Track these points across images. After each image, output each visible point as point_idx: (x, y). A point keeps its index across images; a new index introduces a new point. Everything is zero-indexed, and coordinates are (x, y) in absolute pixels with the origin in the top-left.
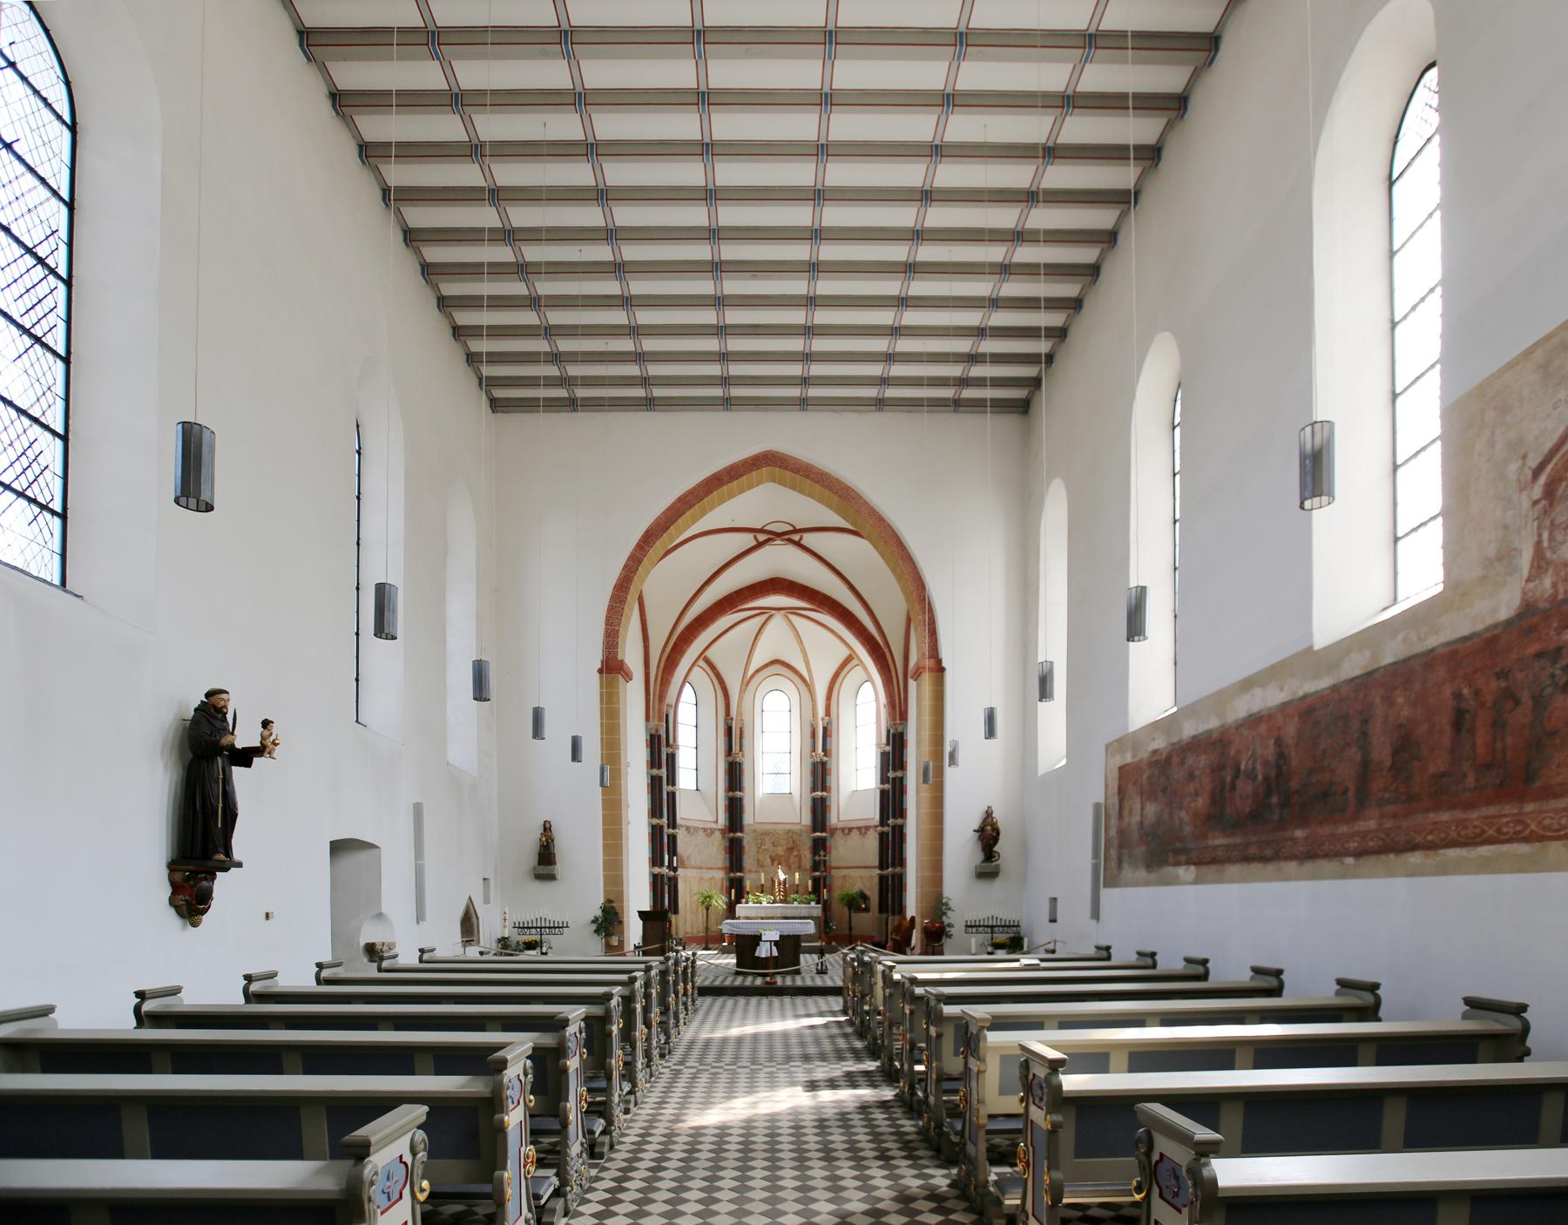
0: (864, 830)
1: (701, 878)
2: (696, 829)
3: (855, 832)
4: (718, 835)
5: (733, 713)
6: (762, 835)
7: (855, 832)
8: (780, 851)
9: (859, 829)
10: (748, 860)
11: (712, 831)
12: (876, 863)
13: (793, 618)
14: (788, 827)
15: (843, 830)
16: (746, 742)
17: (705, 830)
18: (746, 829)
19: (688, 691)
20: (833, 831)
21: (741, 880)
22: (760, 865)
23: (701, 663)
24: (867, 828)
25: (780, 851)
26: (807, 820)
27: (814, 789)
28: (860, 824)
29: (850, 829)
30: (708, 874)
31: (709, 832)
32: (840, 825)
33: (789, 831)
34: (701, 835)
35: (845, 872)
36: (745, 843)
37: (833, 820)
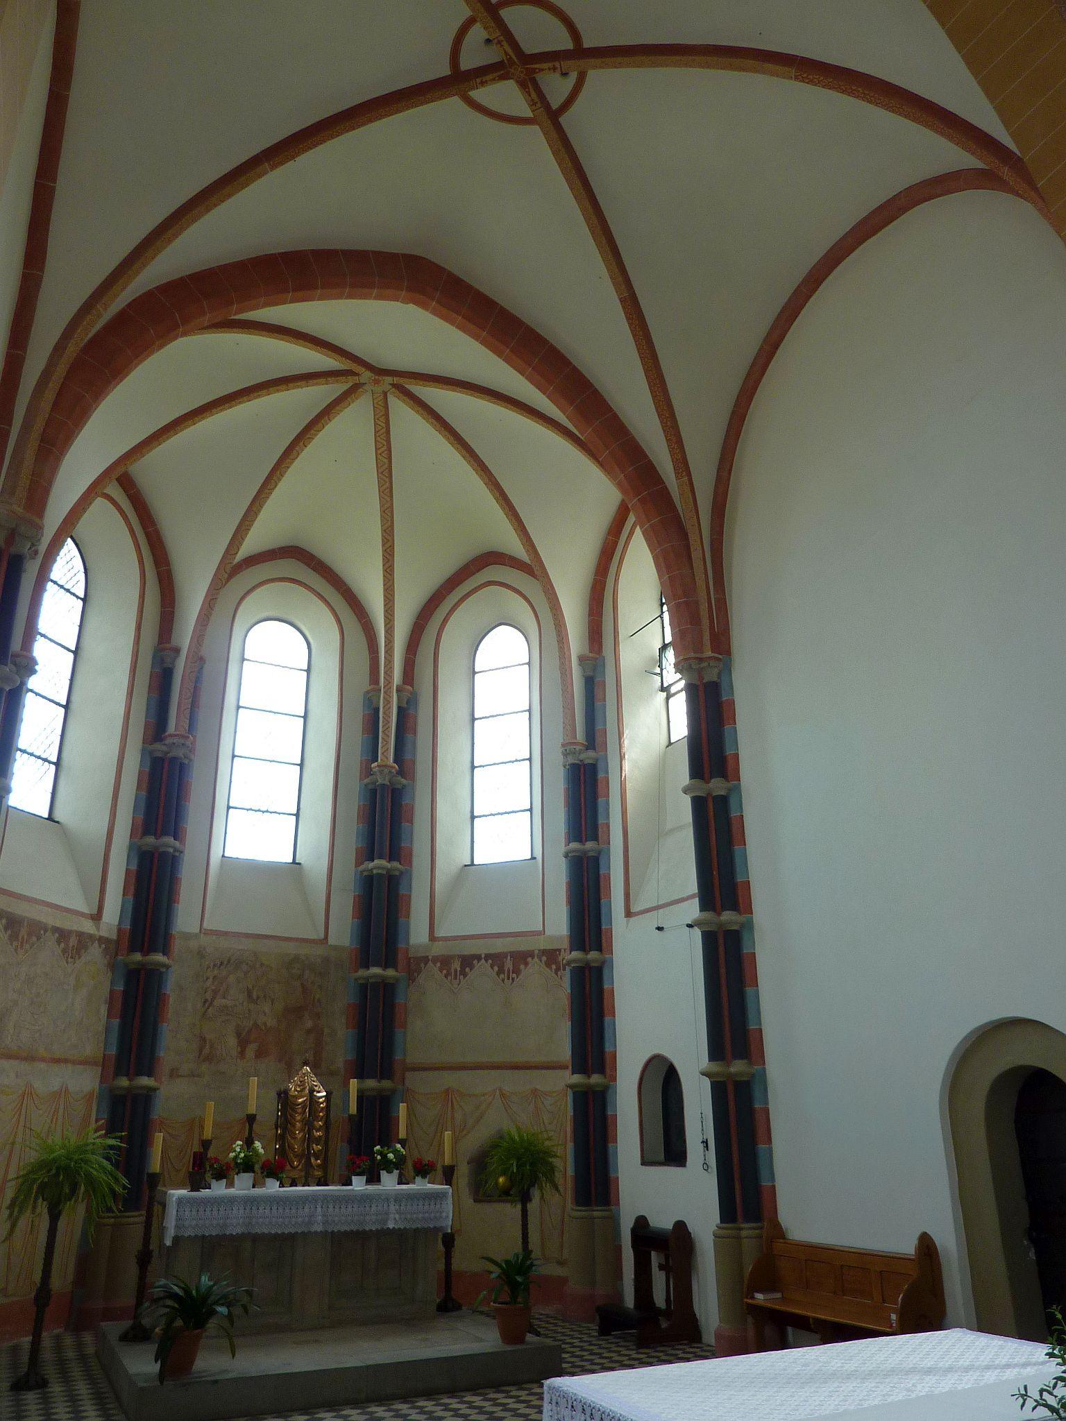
0: (509, 962)
1: (28, 1094)
2: (38, 929)
3: (483, 966)
4: (95, 953)
5: (185, 635)
6: (237, 964)
7: (483, 974)
8: (267, 1015)
9: (496, 959)
10: (174, 1041)
11: (84, 941)
12: (564, 1050)
13: (400, 410)
14: (291, 949)
15: (445, 961)
16: (202, 715)
17: (63, 935)
18: (177, 945)
19: (68, 565)
20: (415, 965)
21: (144, 1100)
22: (206, 1052)
23: (114, 490)
24: (522, 958)
25: (267, 1015)
26: (343, 933)
27: (369, 851)
28: (499, 946)
29: (468, 962)
30: (50, 1080)
31: (73, 944)
32: (437, 950)
33: (296, 959)
34: (49, 951)
35: (450, 1080)
36: (170, 988)
37: (417, 934)
